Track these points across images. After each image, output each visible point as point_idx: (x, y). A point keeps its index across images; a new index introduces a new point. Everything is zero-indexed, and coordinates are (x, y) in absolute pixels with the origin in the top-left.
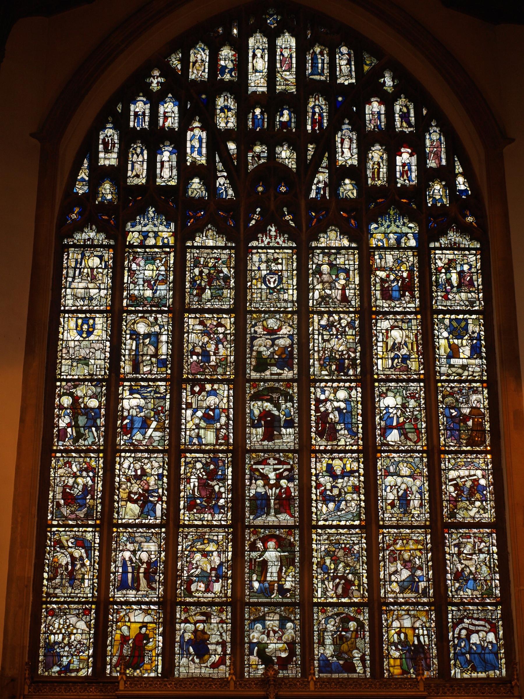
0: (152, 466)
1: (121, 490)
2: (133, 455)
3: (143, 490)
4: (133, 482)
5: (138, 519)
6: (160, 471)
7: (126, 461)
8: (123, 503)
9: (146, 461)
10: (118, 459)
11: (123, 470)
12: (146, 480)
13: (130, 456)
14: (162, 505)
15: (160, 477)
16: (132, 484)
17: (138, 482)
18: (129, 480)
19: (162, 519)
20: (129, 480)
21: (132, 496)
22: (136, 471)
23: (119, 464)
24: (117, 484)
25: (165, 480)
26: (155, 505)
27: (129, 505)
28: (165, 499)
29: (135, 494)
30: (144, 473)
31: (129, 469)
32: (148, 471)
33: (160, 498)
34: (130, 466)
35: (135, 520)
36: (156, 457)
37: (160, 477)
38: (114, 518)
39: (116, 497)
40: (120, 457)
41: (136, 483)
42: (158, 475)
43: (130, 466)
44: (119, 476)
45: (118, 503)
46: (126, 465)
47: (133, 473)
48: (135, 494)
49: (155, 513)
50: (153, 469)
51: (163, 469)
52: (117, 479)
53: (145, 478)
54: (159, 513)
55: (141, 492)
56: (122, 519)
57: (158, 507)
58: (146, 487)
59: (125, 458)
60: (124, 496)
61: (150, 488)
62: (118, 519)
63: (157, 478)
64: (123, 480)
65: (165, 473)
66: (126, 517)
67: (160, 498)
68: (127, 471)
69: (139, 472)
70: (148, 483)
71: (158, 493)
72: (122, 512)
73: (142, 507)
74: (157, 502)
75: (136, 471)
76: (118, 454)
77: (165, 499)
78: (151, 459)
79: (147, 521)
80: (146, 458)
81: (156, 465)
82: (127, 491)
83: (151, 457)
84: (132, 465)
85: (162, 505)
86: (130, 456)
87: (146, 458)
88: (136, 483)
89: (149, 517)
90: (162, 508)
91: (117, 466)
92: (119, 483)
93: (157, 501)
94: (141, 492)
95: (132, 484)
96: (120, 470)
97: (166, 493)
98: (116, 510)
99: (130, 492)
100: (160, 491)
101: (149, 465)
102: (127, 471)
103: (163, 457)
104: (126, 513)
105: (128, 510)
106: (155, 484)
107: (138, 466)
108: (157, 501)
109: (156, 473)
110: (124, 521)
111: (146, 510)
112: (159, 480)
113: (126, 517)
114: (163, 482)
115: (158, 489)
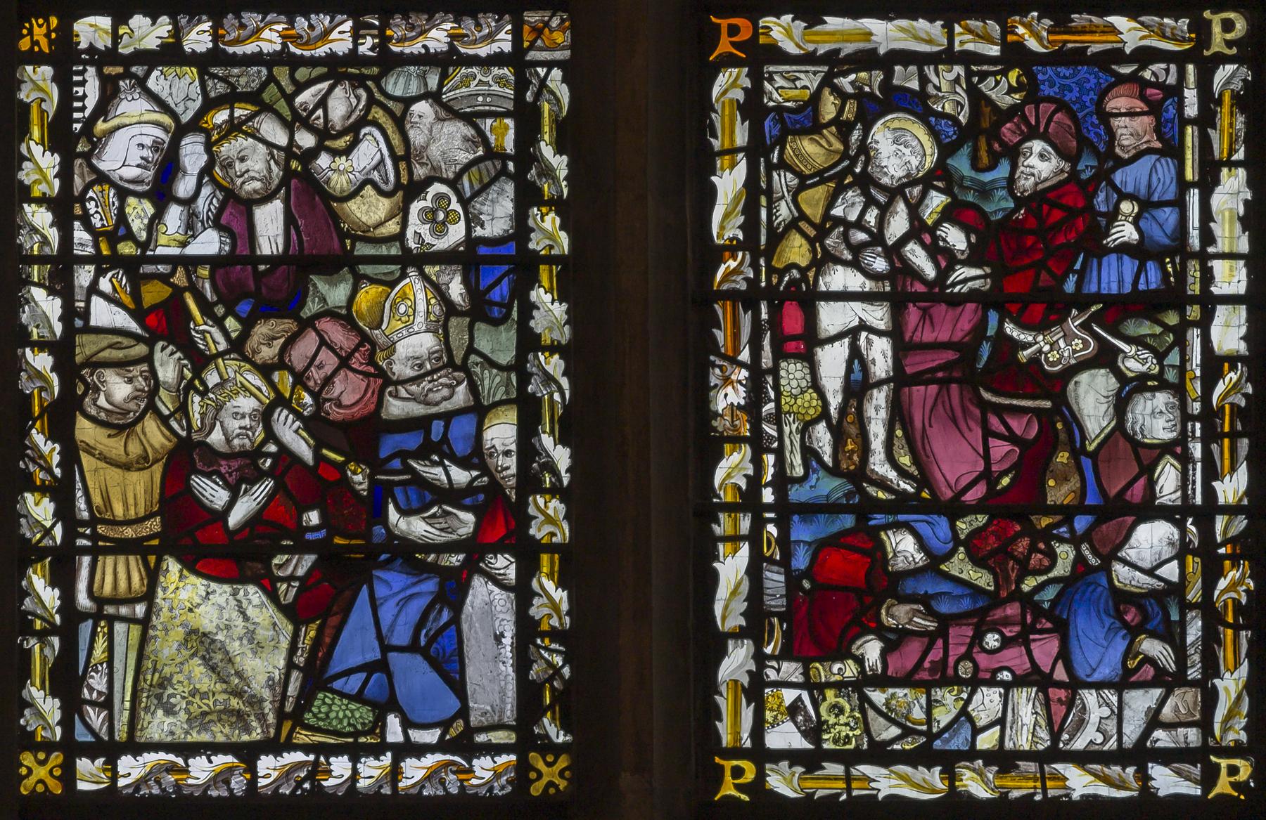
0: (404, 155)
1: (85, 430)
2: (198, 39)
3: (315, 425)
4: (212, 338)
5: (274, 746)
6: (497, 215)
7: (132, 107)
8: (121, 574)
9: (340, 106)
10: (38, 84)
11: (99, 208)
12: (346, 317)
13: (171, 54)
14: (523, 593)
15: (497, 274)
16: (199, 360)
17: (267, 338)
18: (164, 322)
19: (528, 741)
20: (164, 322)
21: (214, 494)
22: (235, 210)
23: (62, 137)
24: (42, 361)
25: (549, 311)
26: (453, 591)
27: (188, 595)
28: (549, 519)
29: (241, 468)
30: (326, 243)
31: (161, 193)
32: (370, 210)
33: (502, 519)
34: (168, 167)
35: (248, 754)
36: (446, 61)
37: (497, 274)
38: (28, 742)
39: (41, 509)
40: (65, 58)
41: (237, 346)
42: (468, 258)
43: (168, 167)
44: (61, 268)
45: (63, 578)
46: (126, 151)
47: (209, 243)
48: (241, 468)
49: (459, 687)
50: (414, 190)
51: (527, 197)
52: (46, 306)
53: (337, 294)
54: (492, 682)
55: (303, 448)
56: (110, 750)
57: (489, 607)
58: (349, 391)
59: (123, 71)
60: (129, 494)
61: (396, 408)
62: (71, 749)
63: (456, 290)
64: (103, 314)
65: (550, 232)
66: (158, 726)
67: (502, 519)
68: (139, 212)
69: (270, 226)
70: (368, 352)
71: (476, 457)
72: (109, 663)
73: (317, 607)
74: (473, 566)
75: (235, 210)
76: (39, 33)
77: (549, 519)
78: (397, 85)
79: (372, 770)
80: (337, 69)
81: (447, 143)
82: (154, 435)
83: (388, 61)
84: (193, 154)
85: (523, 593)
86: (171, 54)
87: (337, 69)
88: (237, 346)
89: (394, 732)
90: (527, 629)
91: (41, 165)
92: (61, 350)
93: (476, 550)
94: (303, 448)
95: (199, 360)
96: (65, 208)
97: (562, 457)
98: (42, 653)
99: (186, 457)
100: (501, 433)
101: (370, 151)
102: (139, 212)
103: (516, 59)
104: (151, 688)
105: (167, 647)
106: (451, 362)
107: (253, 162)
108: (476, 550)
109: (456, 233)
110: (131, 768)
111: (357, 645)
112: (480, 309)
113: (158, 726)
114: (529, 342)
115: (480, 410)
